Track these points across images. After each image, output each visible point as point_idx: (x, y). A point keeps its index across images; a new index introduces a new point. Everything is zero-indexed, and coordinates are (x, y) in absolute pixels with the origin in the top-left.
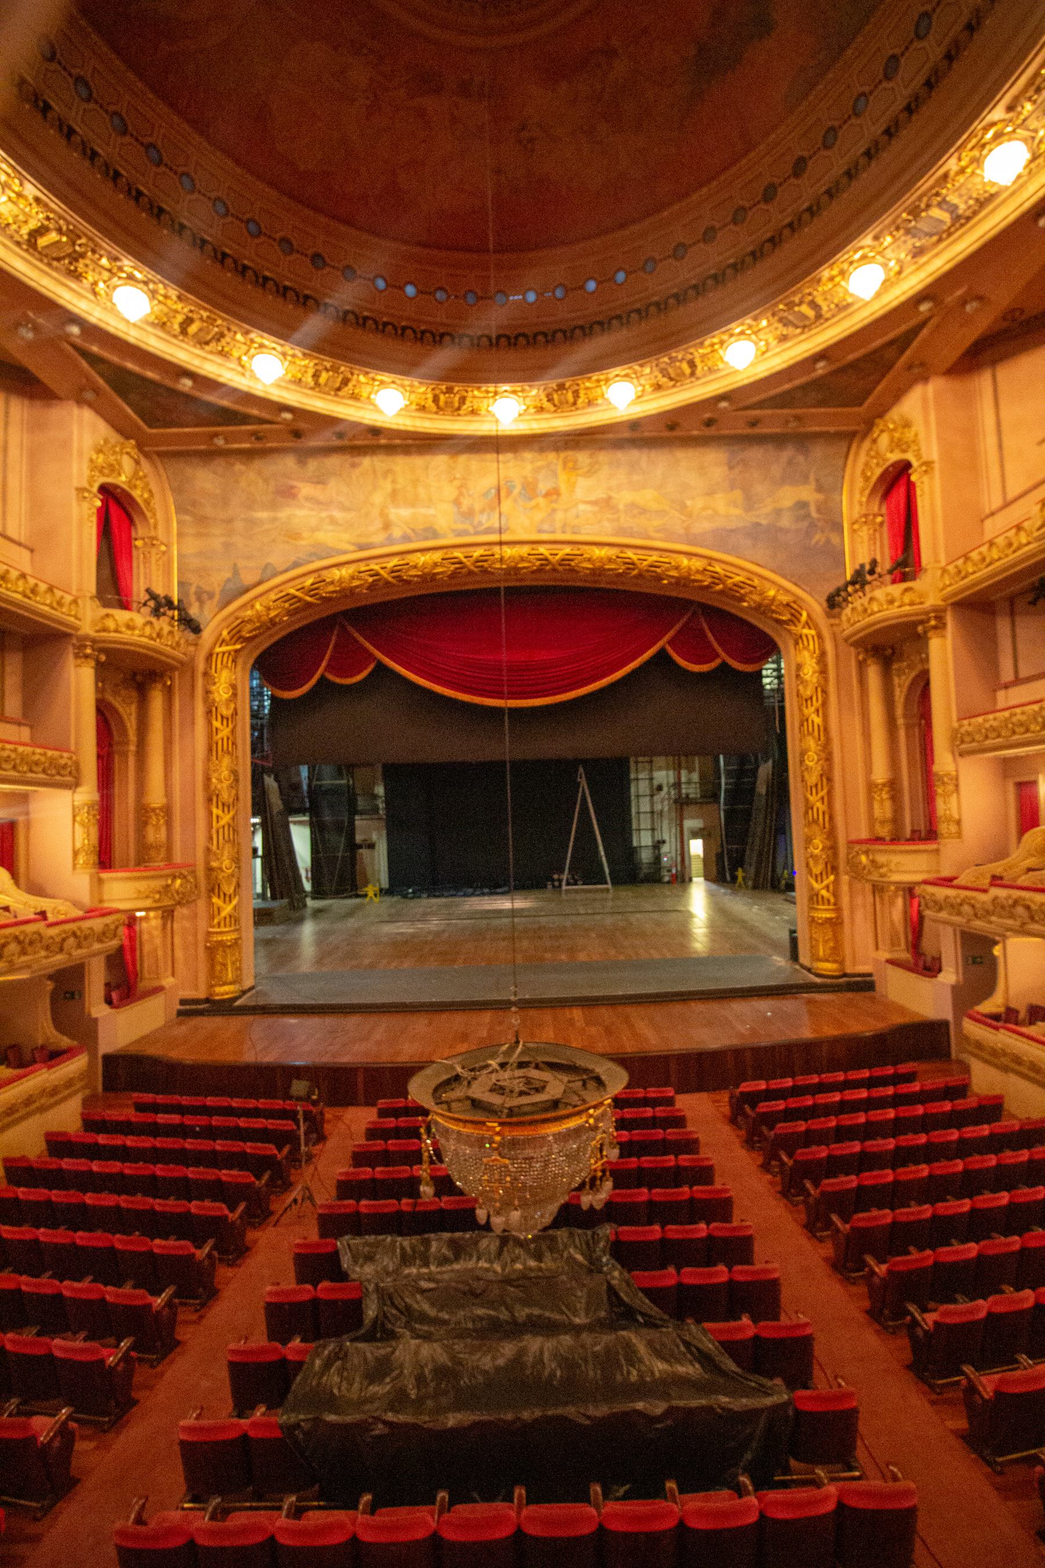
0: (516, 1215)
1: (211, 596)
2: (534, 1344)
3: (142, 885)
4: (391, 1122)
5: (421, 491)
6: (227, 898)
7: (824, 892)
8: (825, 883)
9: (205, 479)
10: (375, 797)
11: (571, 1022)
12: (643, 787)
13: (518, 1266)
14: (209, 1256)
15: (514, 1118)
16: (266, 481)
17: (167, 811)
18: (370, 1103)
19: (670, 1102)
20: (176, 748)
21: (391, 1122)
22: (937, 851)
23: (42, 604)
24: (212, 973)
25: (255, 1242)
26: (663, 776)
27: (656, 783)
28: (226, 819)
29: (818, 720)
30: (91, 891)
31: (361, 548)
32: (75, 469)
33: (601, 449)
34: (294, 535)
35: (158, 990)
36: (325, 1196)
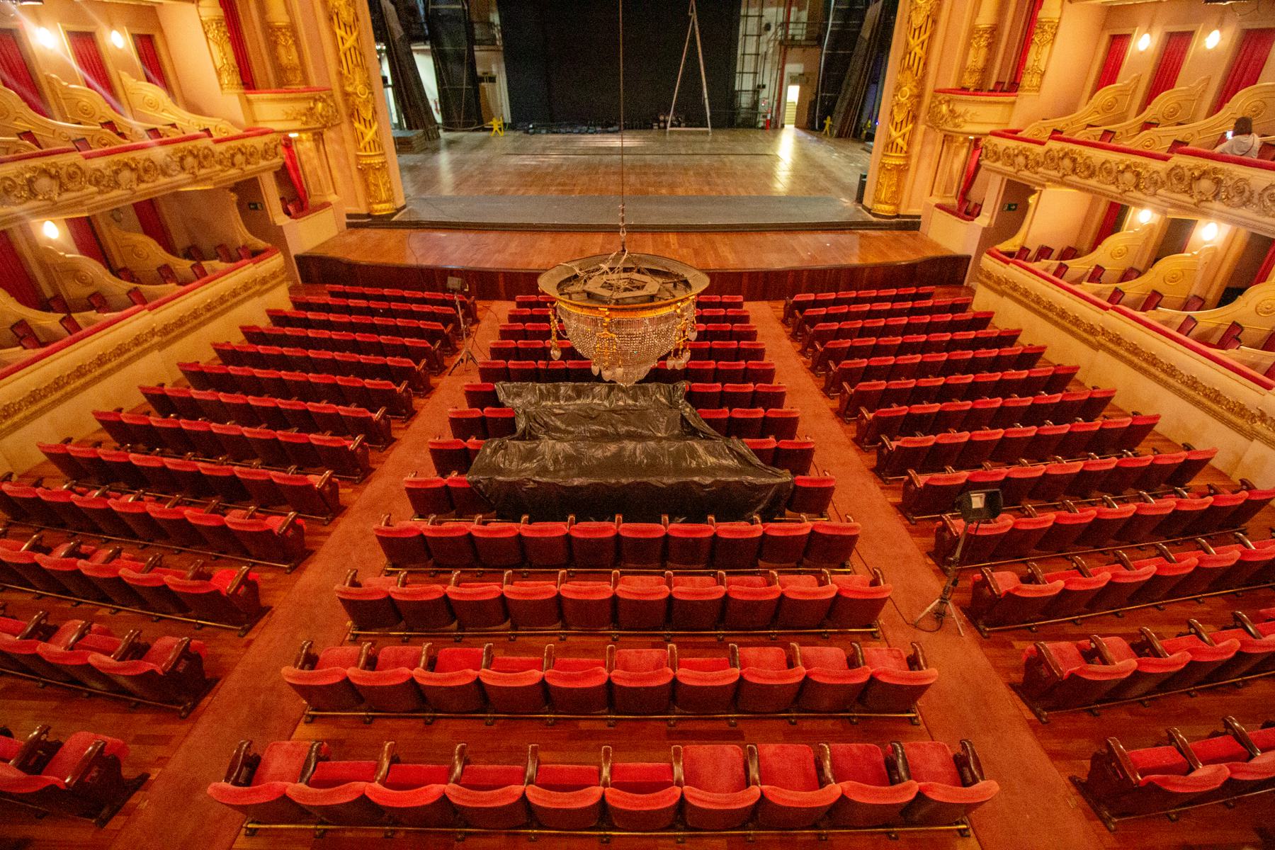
0: (620, 371)
2: (629, 445)
3: (288, 107)
4: (527, 311)
6: (367, 124)
7: (900, 141)
11: (667, 245)
13: (621, 403)
14: (406, 390)
15: (620, 306)
17: (292, 28)
18: (510, 298)
19: (740, 305)
21: (527, 311)
22: (1013, 103)
24: (368, 194)
25: (437, 384)
26: (773, 14)
27: (764, 21)
28: (350, 41)
35: (325, 205)
36: (483, 358)
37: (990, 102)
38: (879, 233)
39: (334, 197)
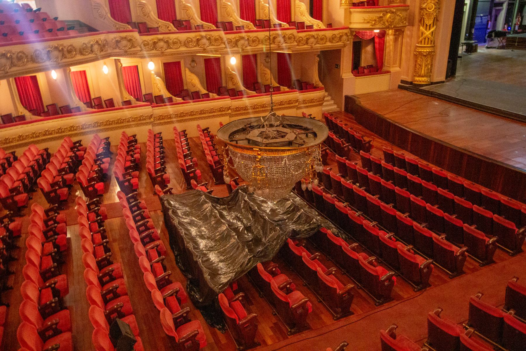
3: (367, 16)
30: (345, 18)
35: (388, 72)
39: (398, 69)
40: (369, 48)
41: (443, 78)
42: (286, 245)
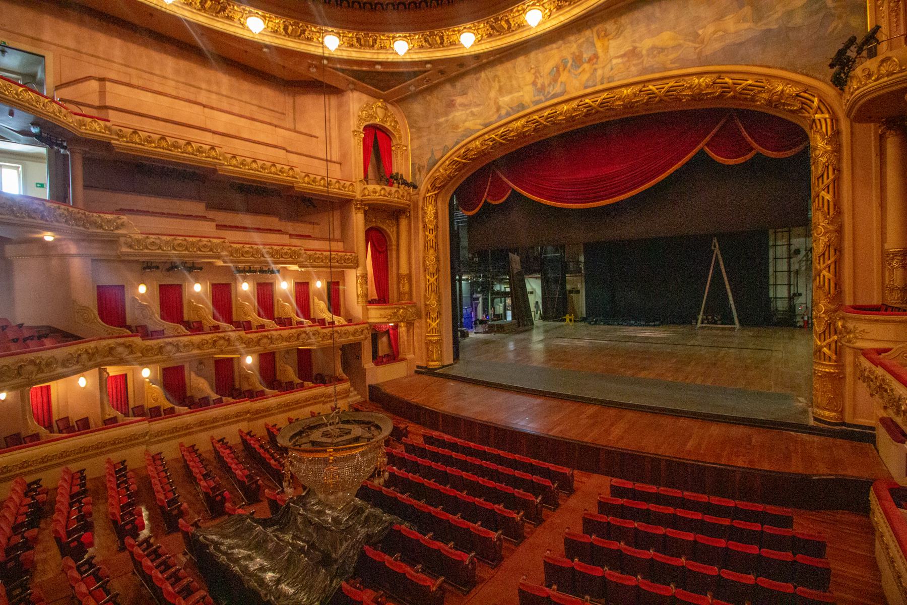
1: (423, 167)
3: (383, 312)
5: (514, 82)
7: (825, 350)
8: (827, 341)
9: (417, 107)
10: (578, 262)
12: (782, 251)
16: (441, 101)
17: (409, 277)
20: (413, 245)
23: (334, 189)
27: (793, 248)
29: (828, 197)
31: (486, 126)
32: (352, 123)
33: (621, 15)
34: (455, 127)
35: (404, 359)
37: (882, 321)
38: (816, 438)
39: (412, 356)
40: (385, 339)
41: (451, 361)
42: (363, 555)
